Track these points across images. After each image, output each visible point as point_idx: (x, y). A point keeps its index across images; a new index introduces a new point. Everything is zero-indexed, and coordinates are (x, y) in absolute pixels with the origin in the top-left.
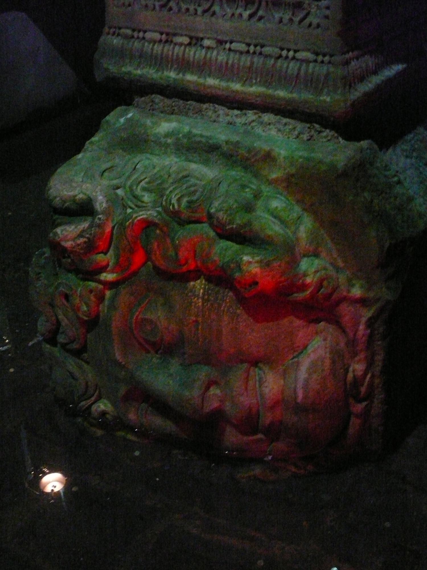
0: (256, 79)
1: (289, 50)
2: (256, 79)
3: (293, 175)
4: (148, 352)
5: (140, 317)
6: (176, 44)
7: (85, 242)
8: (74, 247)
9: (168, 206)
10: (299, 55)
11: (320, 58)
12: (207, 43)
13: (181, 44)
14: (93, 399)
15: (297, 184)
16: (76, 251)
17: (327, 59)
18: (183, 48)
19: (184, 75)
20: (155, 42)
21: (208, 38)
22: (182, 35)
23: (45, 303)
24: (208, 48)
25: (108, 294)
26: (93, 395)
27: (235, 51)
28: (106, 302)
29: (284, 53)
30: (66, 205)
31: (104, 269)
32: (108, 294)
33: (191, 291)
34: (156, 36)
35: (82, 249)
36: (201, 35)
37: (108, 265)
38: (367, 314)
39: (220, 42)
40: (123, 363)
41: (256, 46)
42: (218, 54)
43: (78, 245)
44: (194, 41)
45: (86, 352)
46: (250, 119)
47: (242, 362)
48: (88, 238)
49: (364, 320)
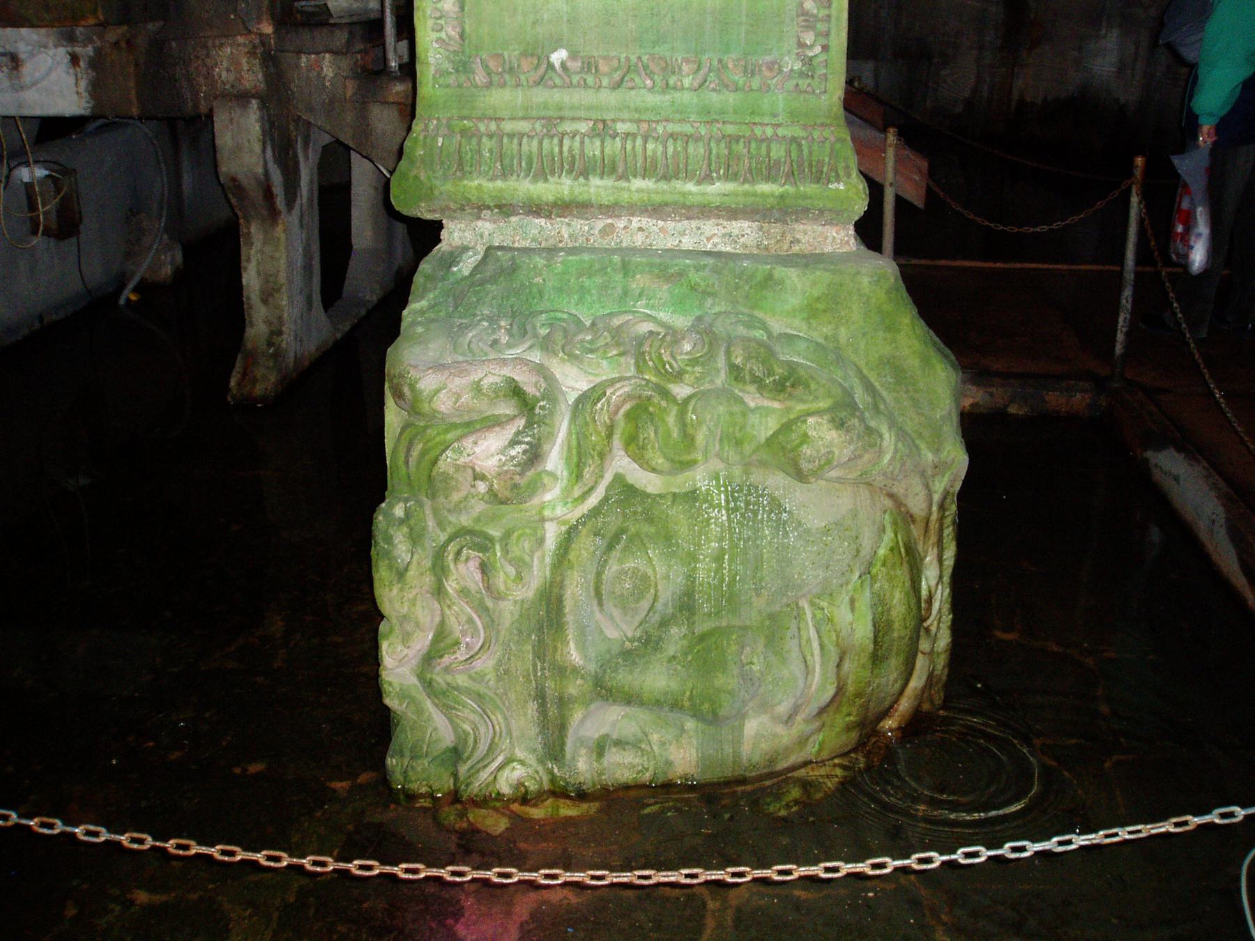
0: (718, 172)
2: (718, 172)
3: (818, 299)
7: (525, 452)
8: (504, 465)
9: (660, 367)
10: (780, 132)
12: (621, 127)
19: (587, 178)
21: (623, 121)
22: (573, 119)
24: (627, 135)
33: (706, 501)
34: (524, 126)
36: (609, 116)
38: (939, 487)
43: (513, 458)
46: (708, 234)
48: (527, 443)
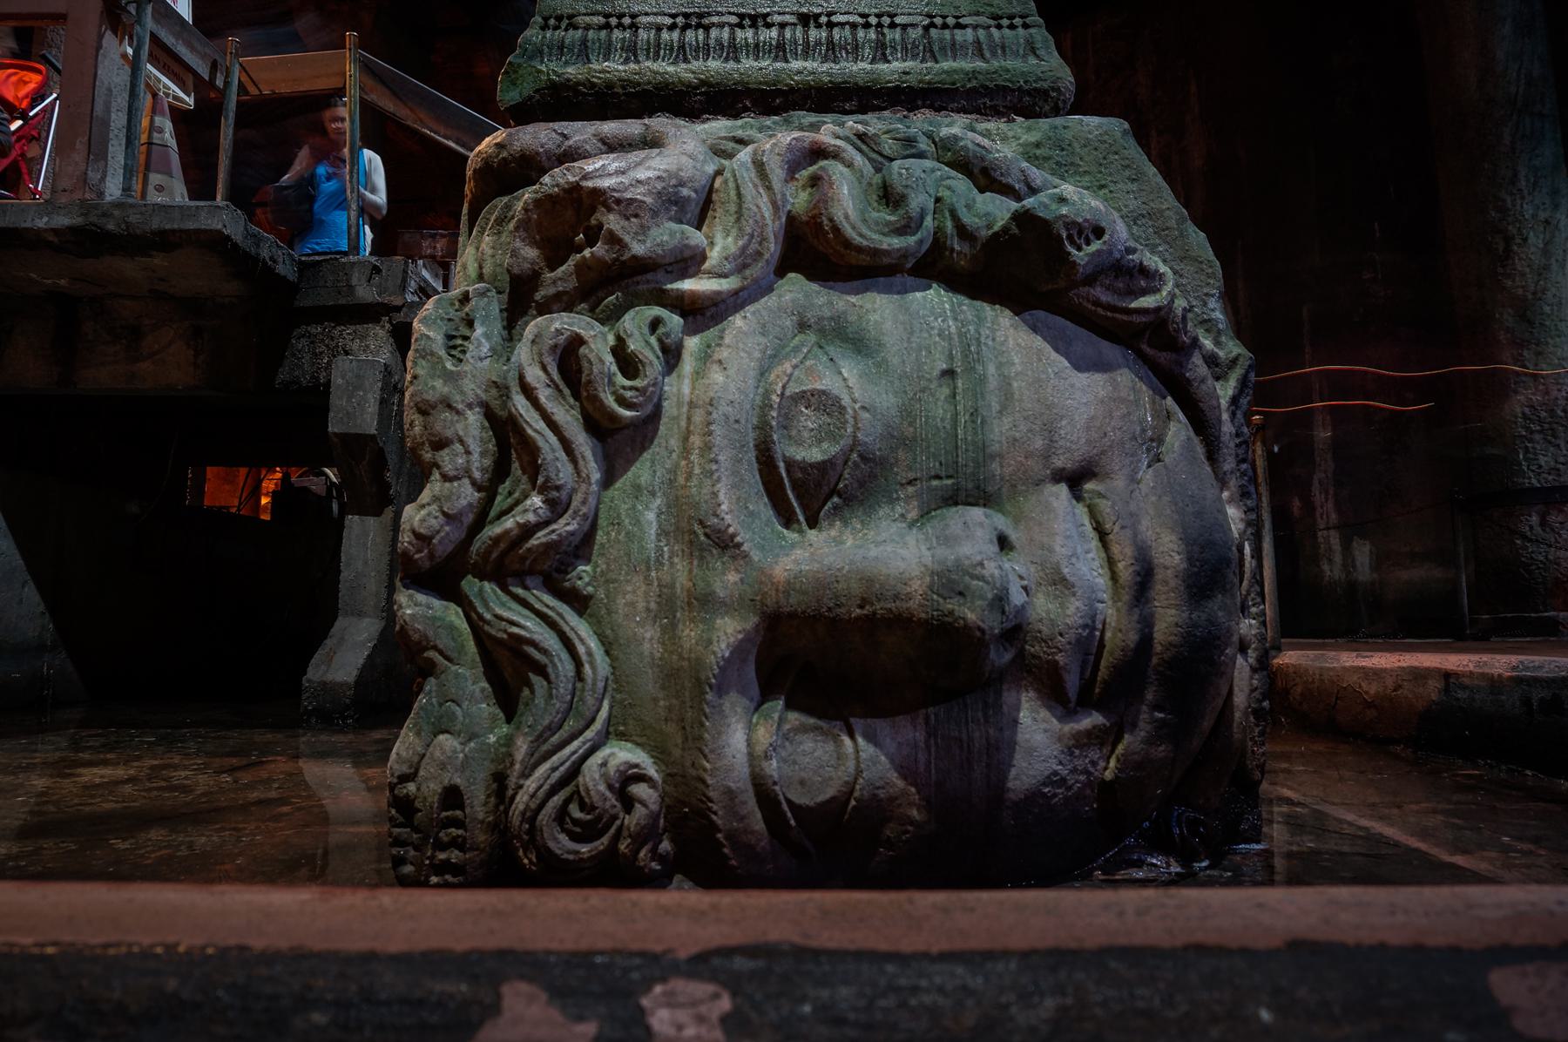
1: (945, 17)
3: (1038, 145)
4: (788, 520)
5: (788, 393)
6: (707, 28)
11: (1005, 22)
12: (777, 19)
13: (721, 26)
14: (589, 734)
15: (1046, 159)
16: (631, 201)
17: (1017, 21)
18: (727, 29)
20: (659, 29)
23: (470, 406)
25: (692, 343)
26: (593, 720)
27: (842, 25)
28: (688, 365)
29: (938, 21)
30: (567, 143)
31: (690, 262)
32: (692, 343)
35: (650, 192)
37: (704, 258)
39: (805, 20)
40: (738, 539)
41: (878, 16)
42: (806, 32)
44: (747, 22)
45: (588, 561)
47: (1059, 476)
49: (1224, 403)
